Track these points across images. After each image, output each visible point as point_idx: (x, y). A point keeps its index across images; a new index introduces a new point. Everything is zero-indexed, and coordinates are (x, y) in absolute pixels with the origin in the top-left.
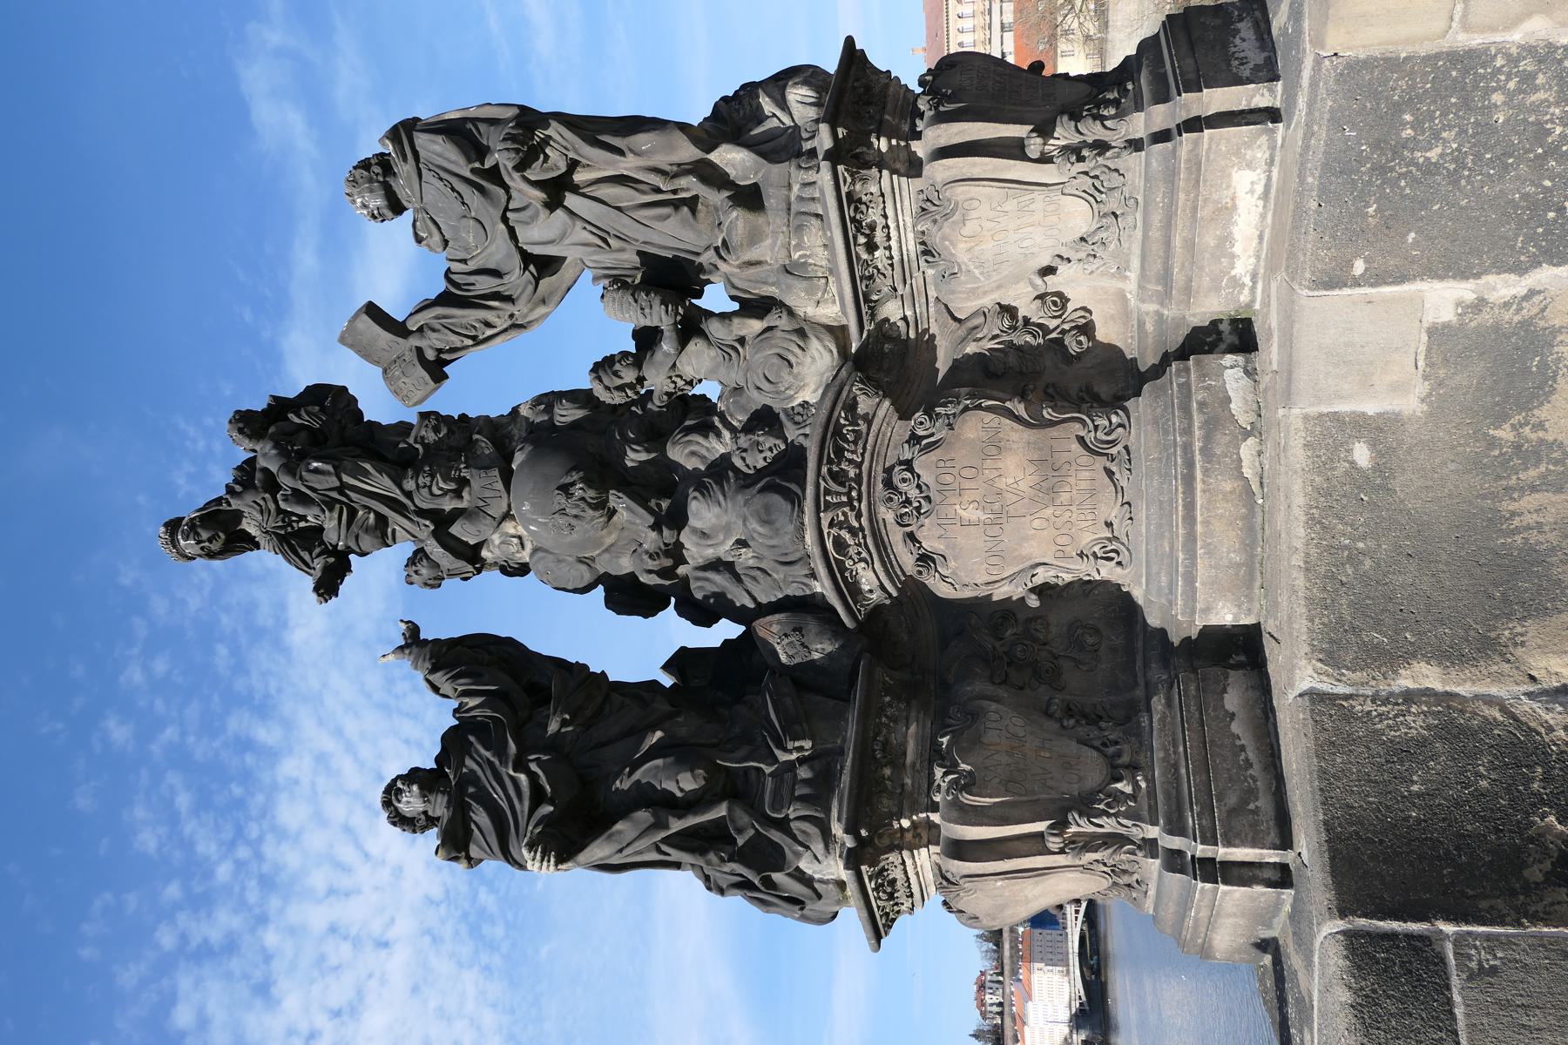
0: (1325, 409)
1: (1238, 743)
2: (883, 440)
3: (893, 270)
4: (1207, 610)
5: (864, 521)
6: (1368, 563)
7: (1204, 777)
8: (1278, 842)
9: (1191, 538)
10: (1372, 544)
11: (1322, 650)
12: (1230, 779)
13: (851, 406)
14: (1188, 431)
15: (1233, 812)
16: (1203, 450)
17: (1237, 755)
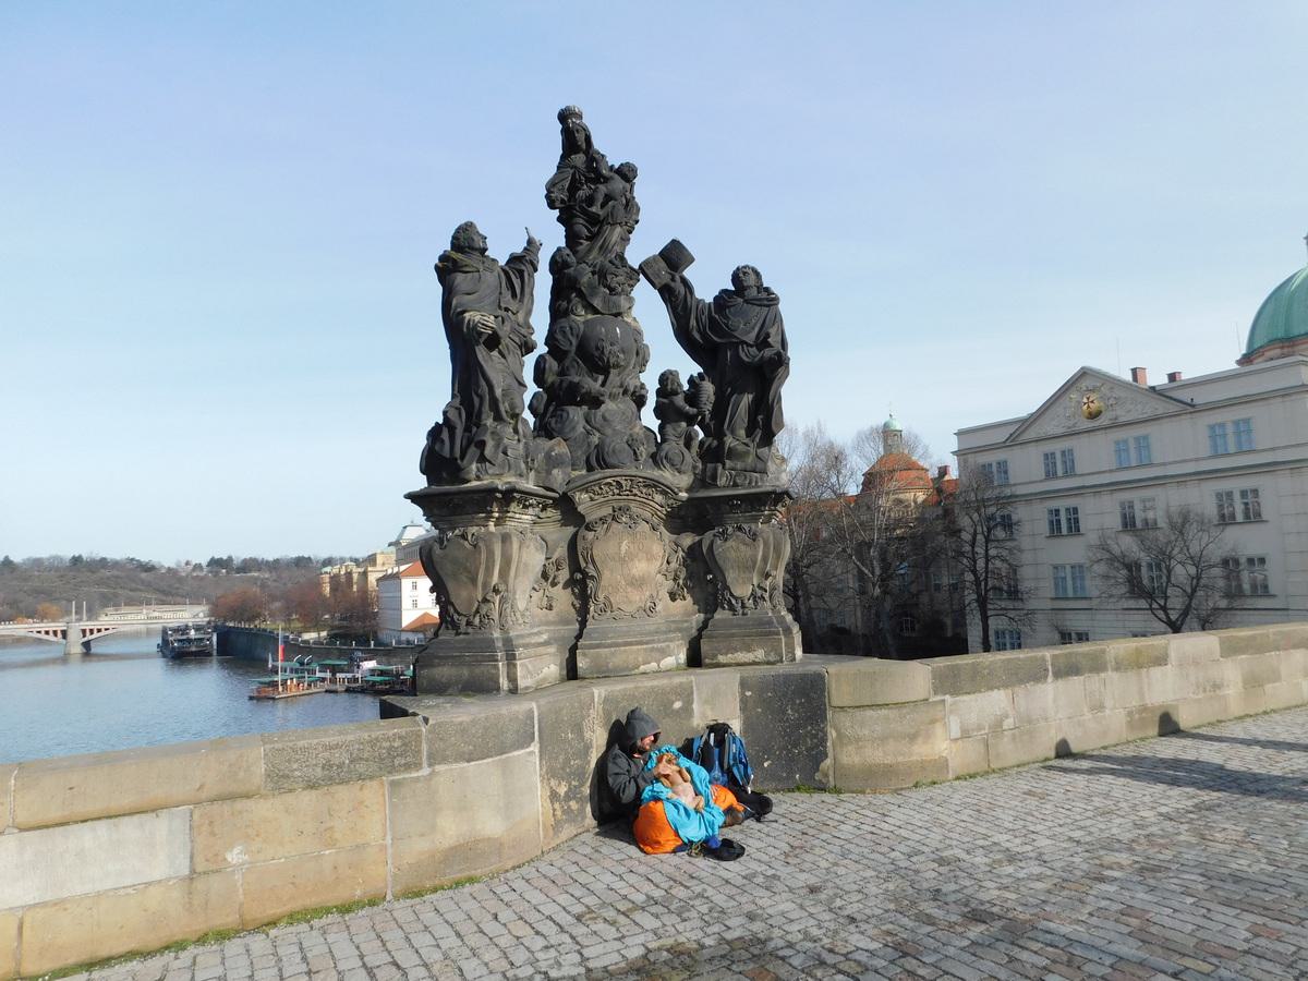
4: (584, 655)
14: (659, 641)
16: (652, 649)
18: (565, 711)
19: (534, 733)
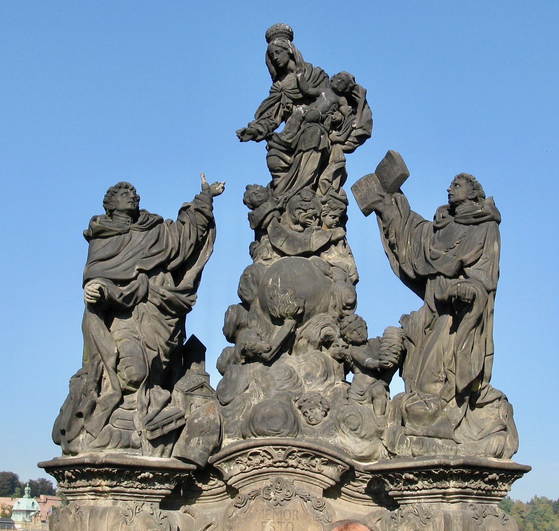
2: (312, 480)
3: (398, 491)
5: (265, 469)
13: (329, 463)
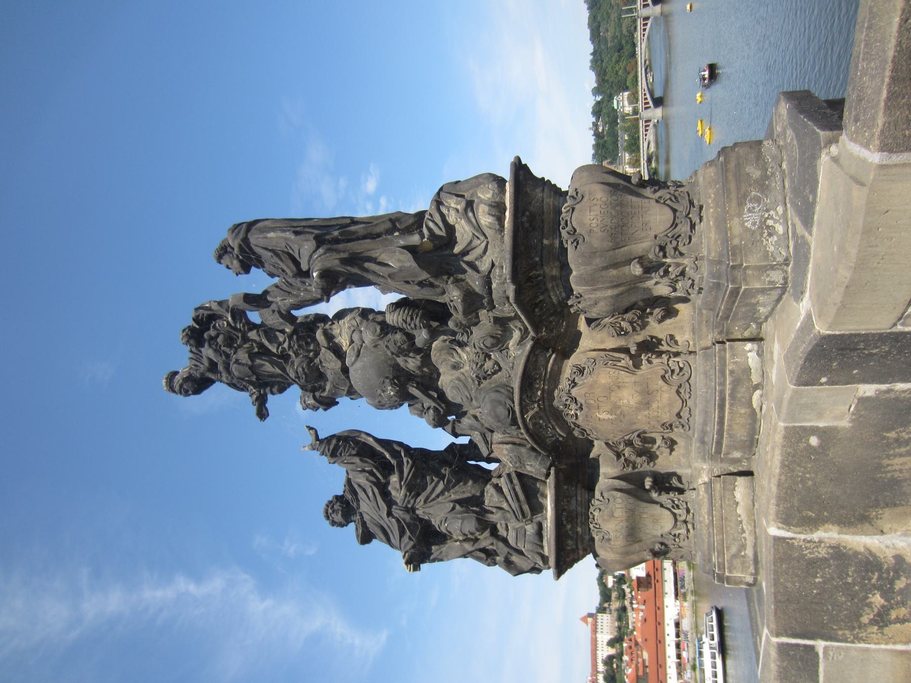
0: (797, 425)
1: (739, 519)
6: (810, 483)
7: (721, 537)
8: (753, 571)
9: (720, 432)
10: (813, 475)
11: (782, 518)
12: (734, 539)
14: (723, 384)
15: (734, 556)
16: (732, 396)
17: (737, 526)
18: (789, 585)
19: (805, 646)
